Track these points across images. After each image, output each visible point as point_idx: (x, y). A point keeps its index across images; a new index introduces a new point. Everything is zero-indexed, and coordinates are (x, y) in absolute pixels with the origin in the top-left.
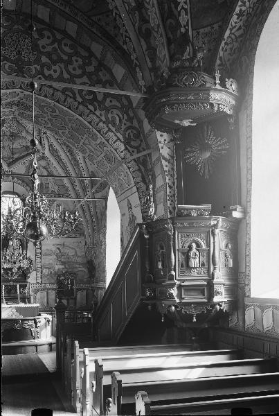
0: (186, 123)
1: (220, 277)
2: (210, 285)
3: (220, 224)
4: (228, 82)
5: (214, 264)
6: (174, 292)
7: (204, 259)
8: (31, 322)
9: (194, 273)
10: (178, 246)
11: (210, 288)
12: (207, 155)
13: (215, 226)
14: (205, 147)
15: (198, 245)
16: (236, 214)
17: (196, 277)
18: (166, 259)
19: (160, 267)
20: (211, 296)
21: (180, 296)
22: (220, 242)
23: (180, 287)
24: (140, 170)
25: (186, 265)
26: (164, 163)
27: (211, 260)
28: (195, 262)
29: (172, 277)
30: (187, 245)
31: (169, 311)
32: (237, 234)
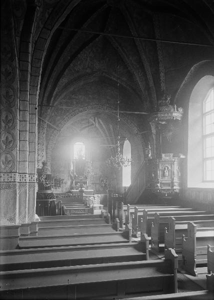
0: (164, 123)
1: (176, 180)
2: (172, 183)
3: (176, 160)
4: (179, 109)
5: (174, 175)
6: (159, 185)
7: (170, 173)
8: (93, 198)
9: (166, 178)
10: (160, 168)
11: (172, 184)
12: (171, 133)
13: (174, 161)
14: (169, 131)
15: (168, 168)
16: (182, 157)
17: (167, 180)
18: (156, 175)
19: (153, 175)
20: (173, 187)
21: (161, 186)
22: (176, 168)
23: (161, 183)
24: (143, 138)
25: (164, 175)
26: (154, 136)
27: (172, 173)
28: (167, 174)
29: (158, 180)
30: (164, 167)
31: (157, 192)
32: (183, 165)
